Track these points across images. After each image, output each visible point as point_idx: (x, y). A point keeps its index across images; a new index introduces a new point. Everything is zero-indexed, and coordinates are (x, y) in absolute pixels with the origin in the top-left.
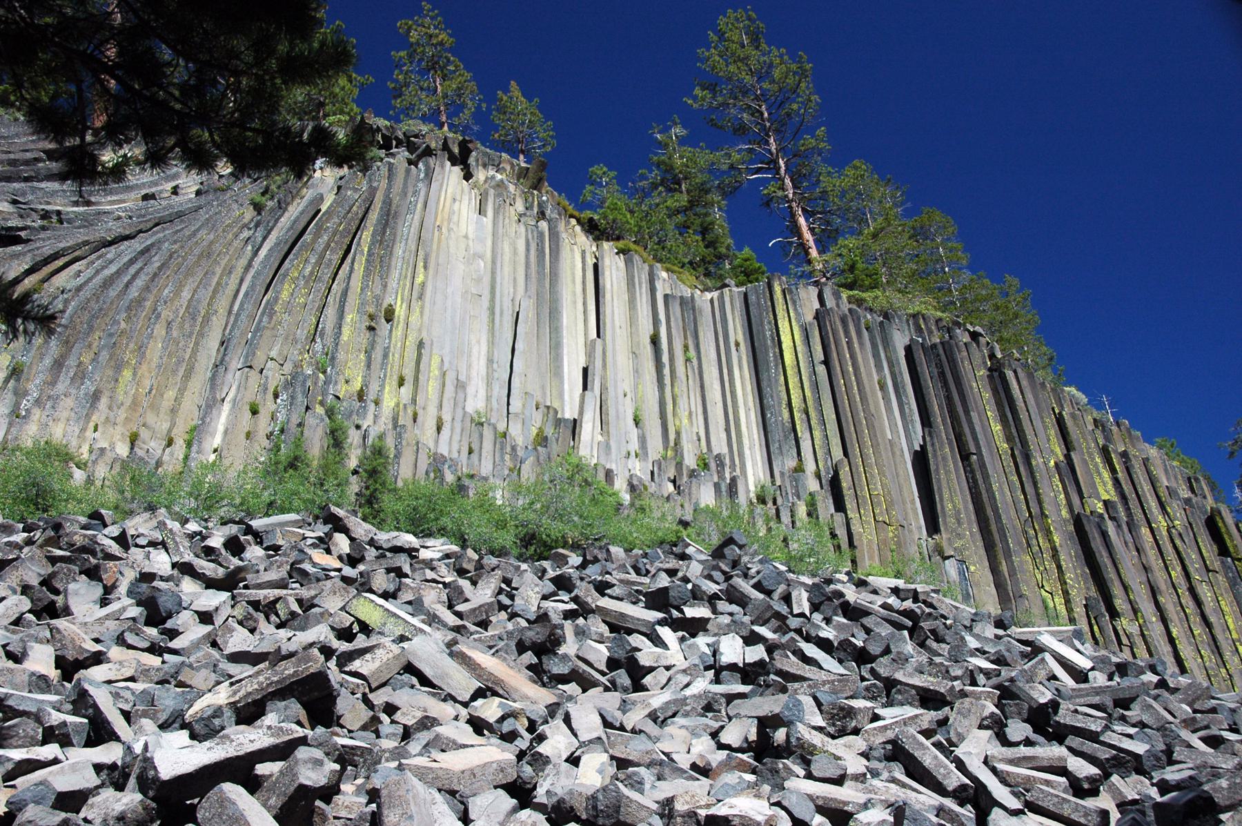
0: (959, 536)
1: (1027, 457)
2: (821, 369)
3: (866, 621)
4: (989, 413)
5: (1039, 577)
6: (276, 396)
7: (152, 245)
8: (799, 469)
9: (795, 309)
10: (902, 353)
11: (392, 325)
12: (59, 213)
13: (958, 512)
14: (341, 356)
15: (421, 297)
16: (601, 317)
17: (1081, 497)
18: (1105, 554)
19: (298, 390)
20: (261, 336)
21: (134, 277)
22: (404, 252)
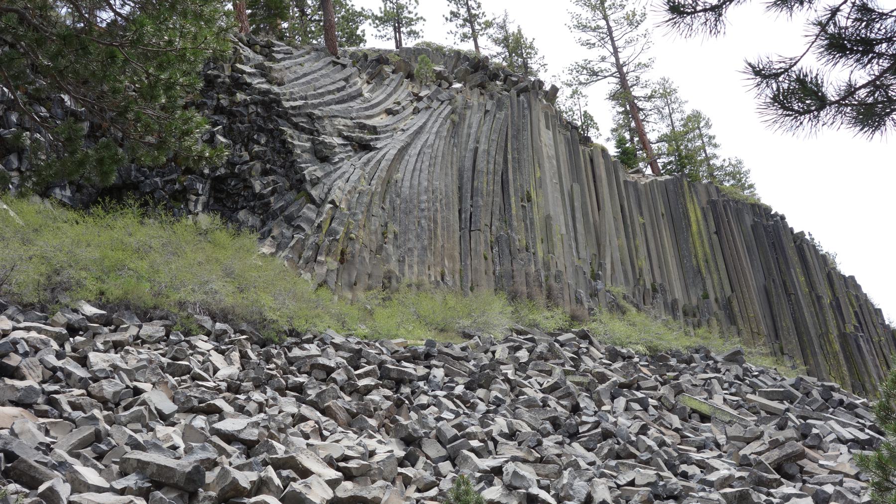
0: (791, 342)
1: (819, 298)
2: (715, 237)
3: (856, 410)
4: (798, 270)
5: (828, 368)
6: (492, 249)
7: (420, 150)
8: (706, 296)
9: (697, 197)
10: (750, 229)
11: (531, 204)
12: (375, 128)
13: (788, 328)
14: (515, 223)
15: (540, 187)
16: (600, 195)
17: (844, 323)
18: (859, 357)
19: (504, 245)
20: (481, 210)
21: (421, 171)
22: (528, 156)
